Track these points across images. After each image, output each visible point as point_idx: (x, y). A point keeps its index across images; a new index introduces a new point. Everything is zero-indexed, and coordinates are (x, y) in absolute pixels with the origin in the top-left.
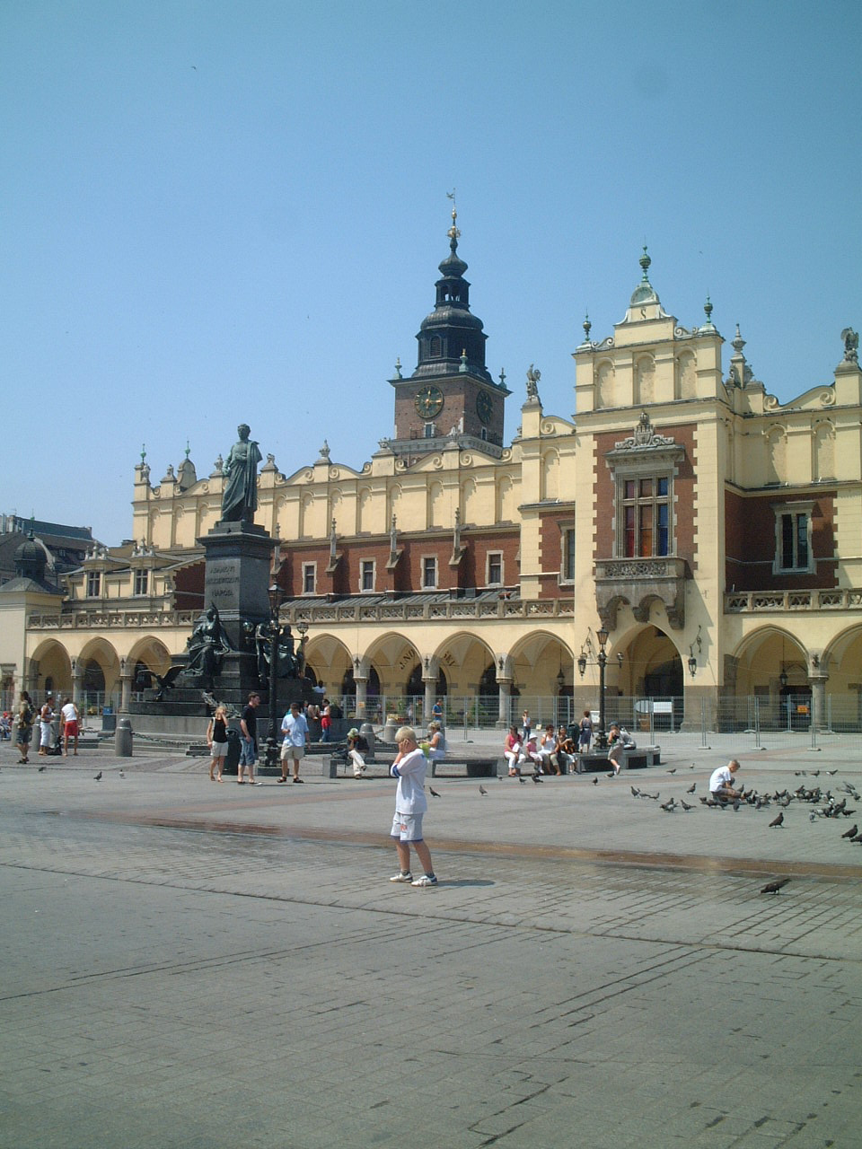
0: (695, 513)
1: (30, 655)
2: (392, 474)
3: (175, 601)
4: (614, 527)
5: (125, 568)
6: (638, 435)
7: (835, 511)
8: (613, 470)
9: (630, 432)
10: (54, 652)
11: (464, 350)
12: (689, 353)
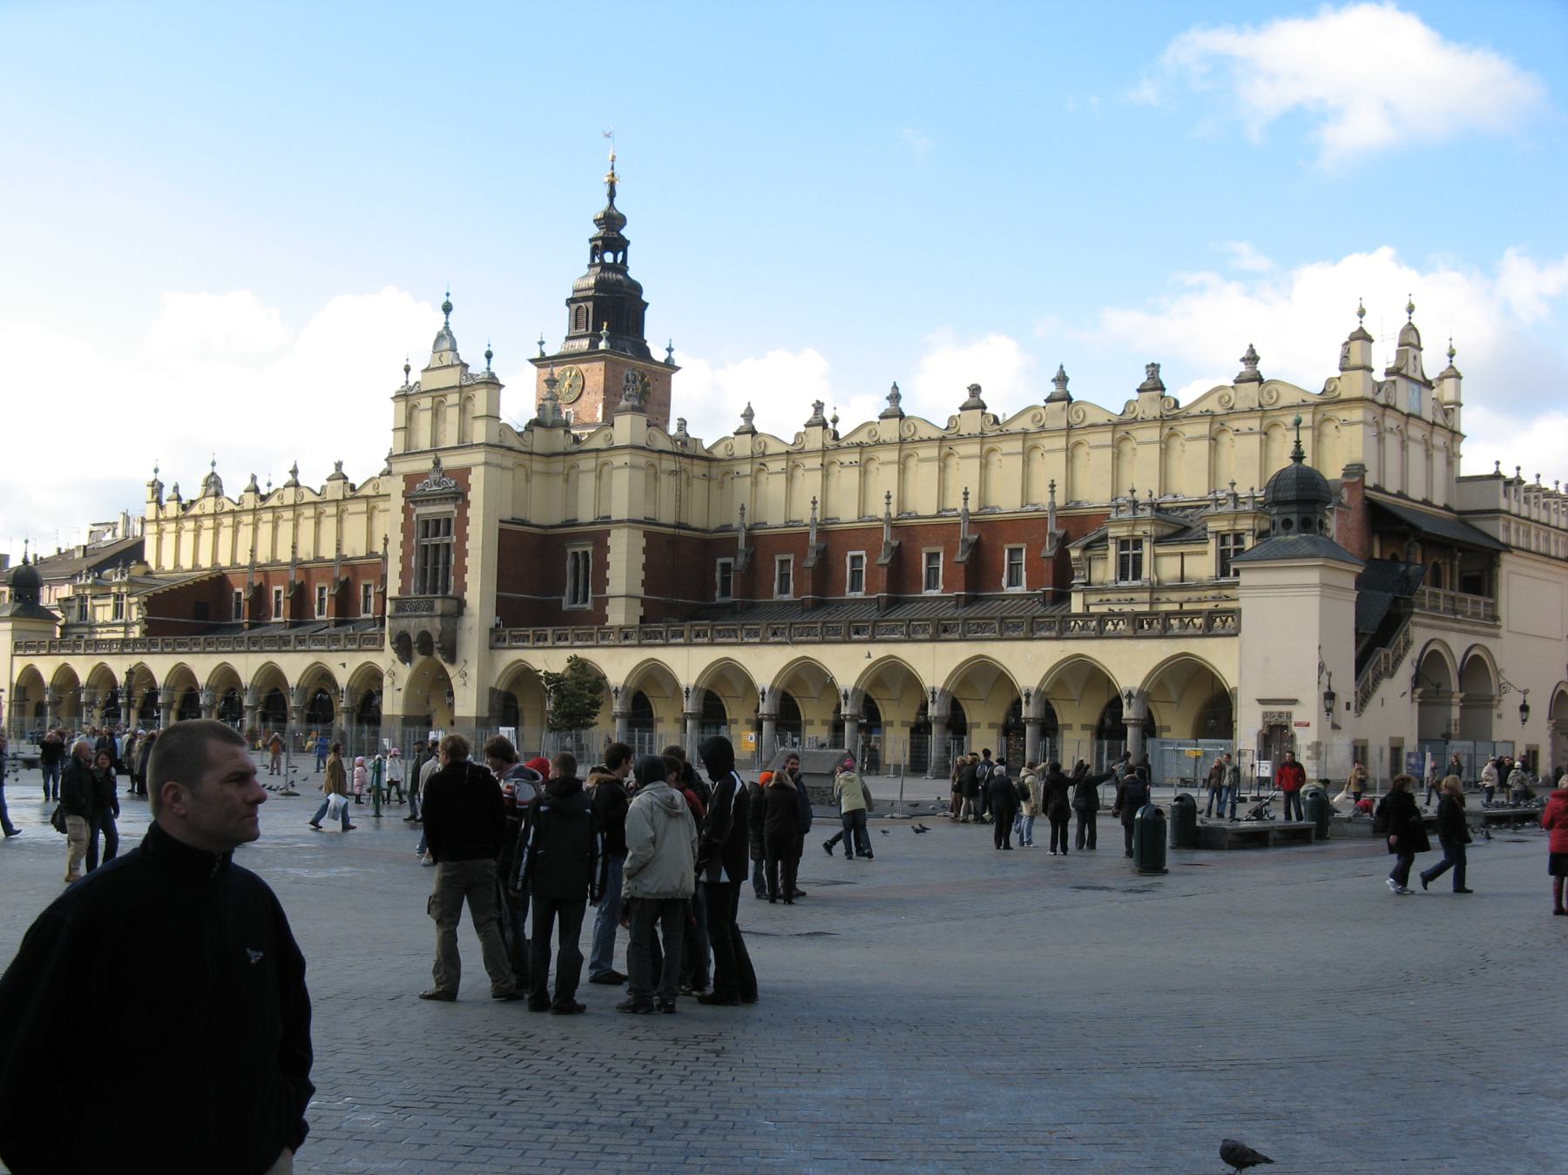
0: (465, 553)
1: (15, 681)
2: (341, 497)
3: (146, 626)
4: (413, 566)
5: (107, 595)
6: (436, 476)
7: (607, 549)
8: (414, 510)
9: (424, 475)
10: (32, 675)
11: (605, 324)
12: (469, 398)
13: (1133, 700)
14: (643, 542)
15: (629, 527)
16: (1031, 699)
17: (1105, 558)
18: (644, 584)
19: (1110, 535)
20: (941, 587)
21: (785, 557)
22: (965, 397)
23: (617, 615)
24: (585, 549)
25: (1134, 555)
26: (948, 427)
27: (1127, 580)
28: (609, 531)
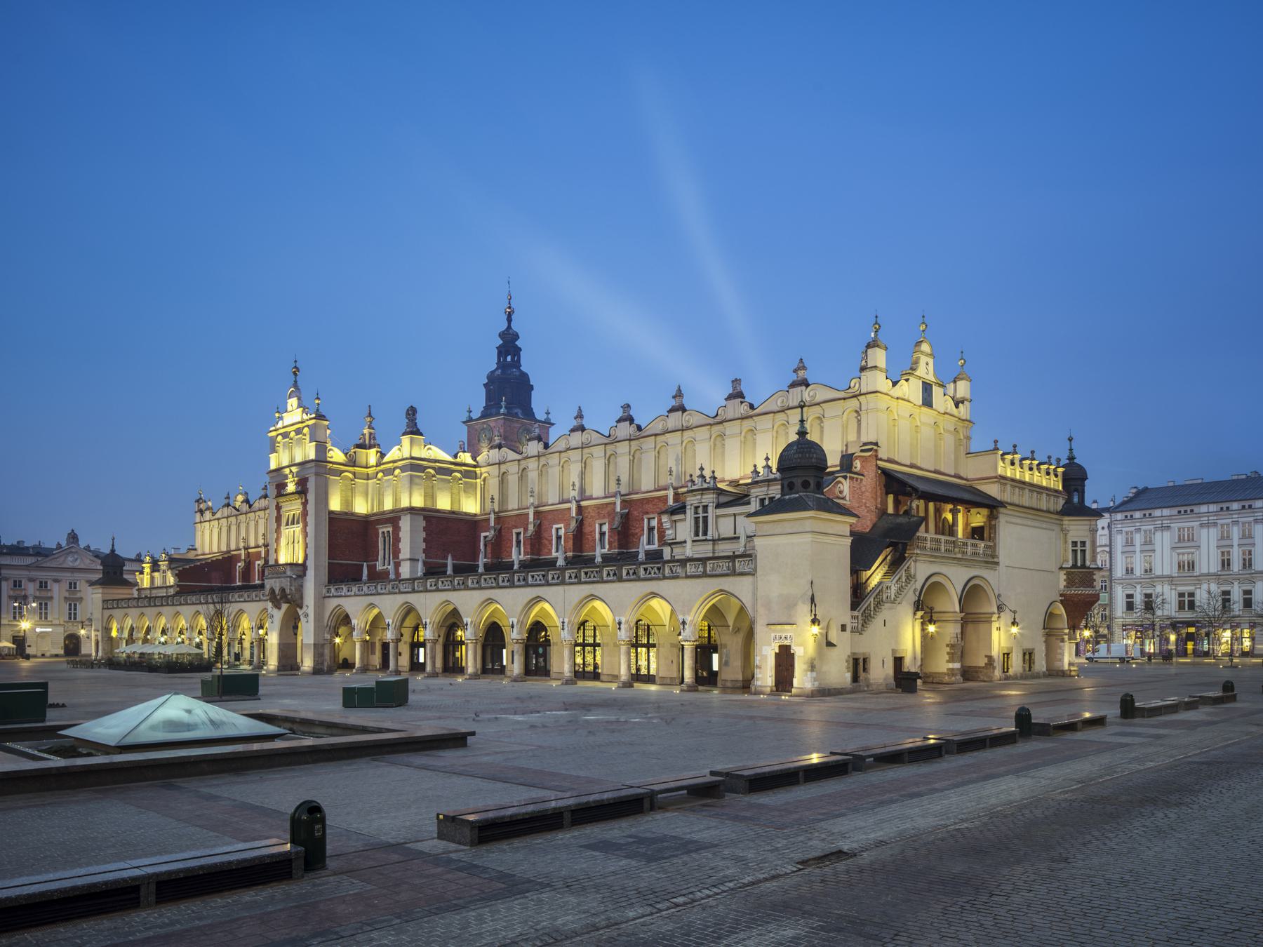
3: (178, 589)
13: (686, 626)
14: (424, 524)
15: (411, 513)
16: (622, 626)
17: (685, 520)
18: (424, 551)
19: (688, 503)
20: (607, 547)
21: (518, 530)
22: (620, 413)
23: (405, 570)
24: (388, 529)
25: (703, 517)
26: (610, 436)
27: (698, 536)
28: (400, 516)
